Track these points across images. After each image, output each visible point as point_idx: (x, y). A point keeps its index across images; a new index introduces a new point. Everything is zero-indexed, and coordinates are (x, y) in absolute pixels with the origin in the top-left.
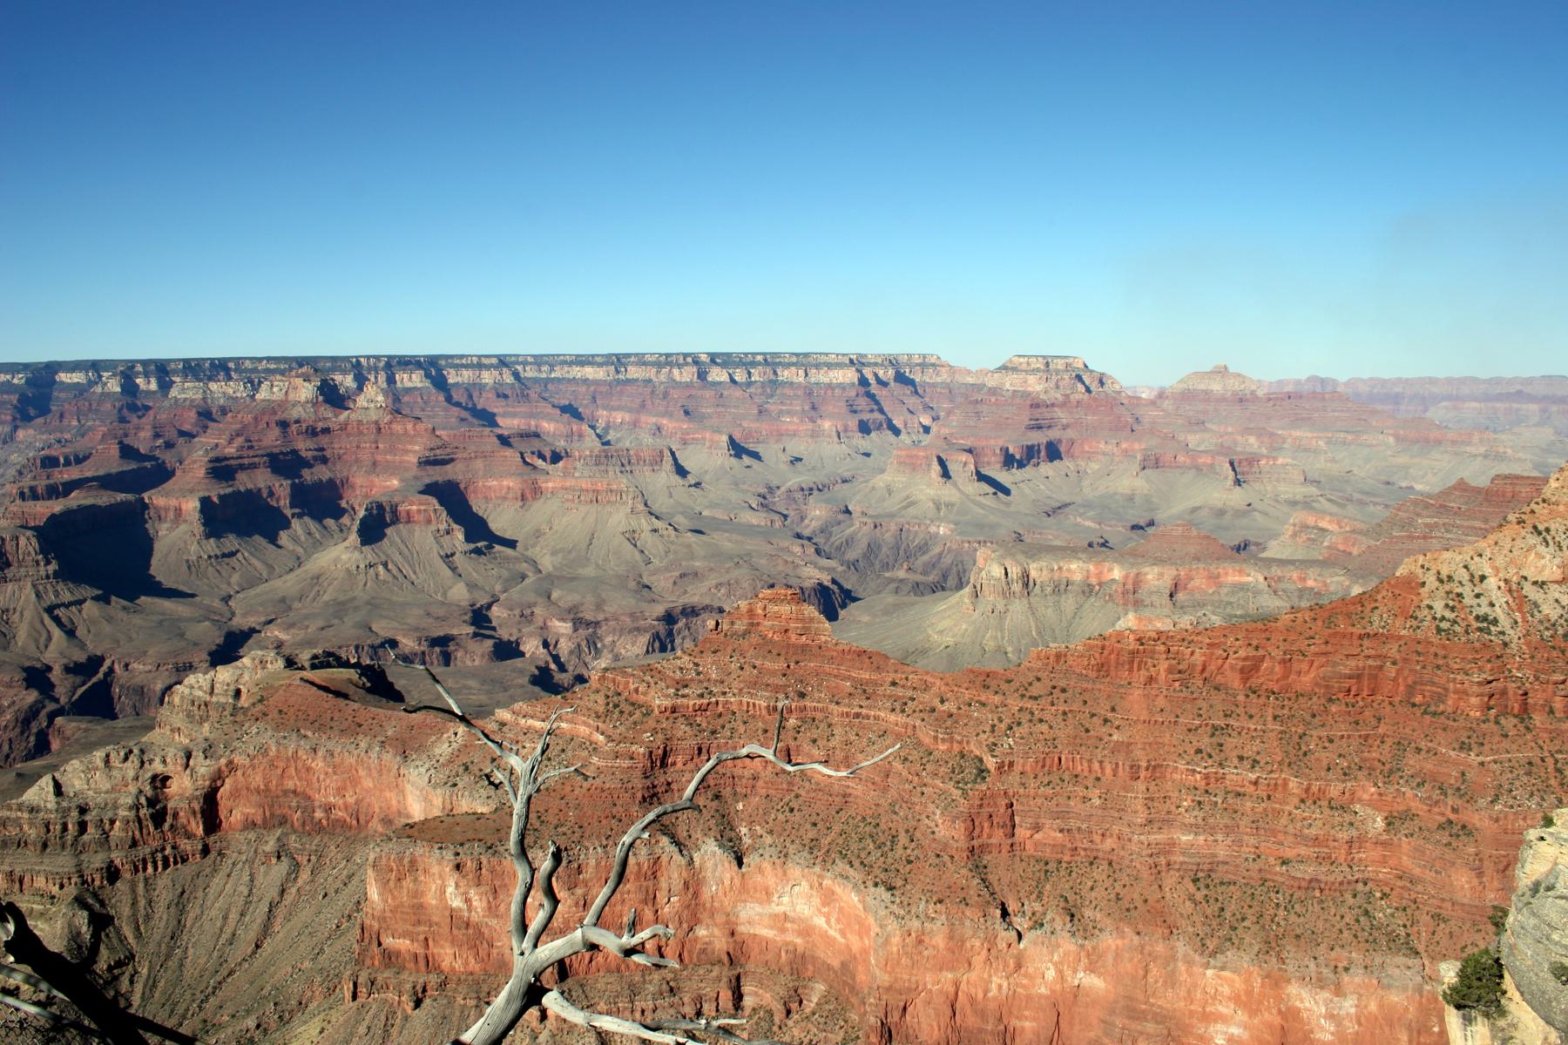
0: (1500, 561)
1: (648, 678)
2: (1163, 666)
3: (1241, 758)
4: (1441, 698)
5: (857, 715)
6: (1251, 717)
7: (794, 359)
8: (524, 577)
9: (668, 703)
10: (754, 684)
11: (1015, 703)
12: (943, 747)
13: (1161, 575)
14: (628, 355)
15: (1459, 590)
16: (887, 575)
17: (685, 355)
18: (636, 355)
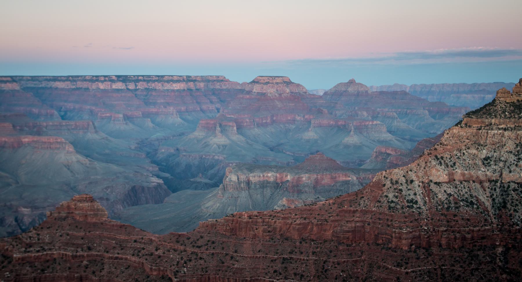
0: (420, 174)
1: (14, 243)
2: (261, 229)
3: (295, 274)
4: (390, 241)
5: (117, 258)
6: (302, 253)
7: (157, 78)
8: (9, 185)
9: (19, 256)
10: (67, 244)
11: (190, 249)
12: (155, 273)
13: (309, 178)
14: (78, 76)
15: (401, 188)
16: (192, 180)
17: (105, 76)
18: (81, 76)
